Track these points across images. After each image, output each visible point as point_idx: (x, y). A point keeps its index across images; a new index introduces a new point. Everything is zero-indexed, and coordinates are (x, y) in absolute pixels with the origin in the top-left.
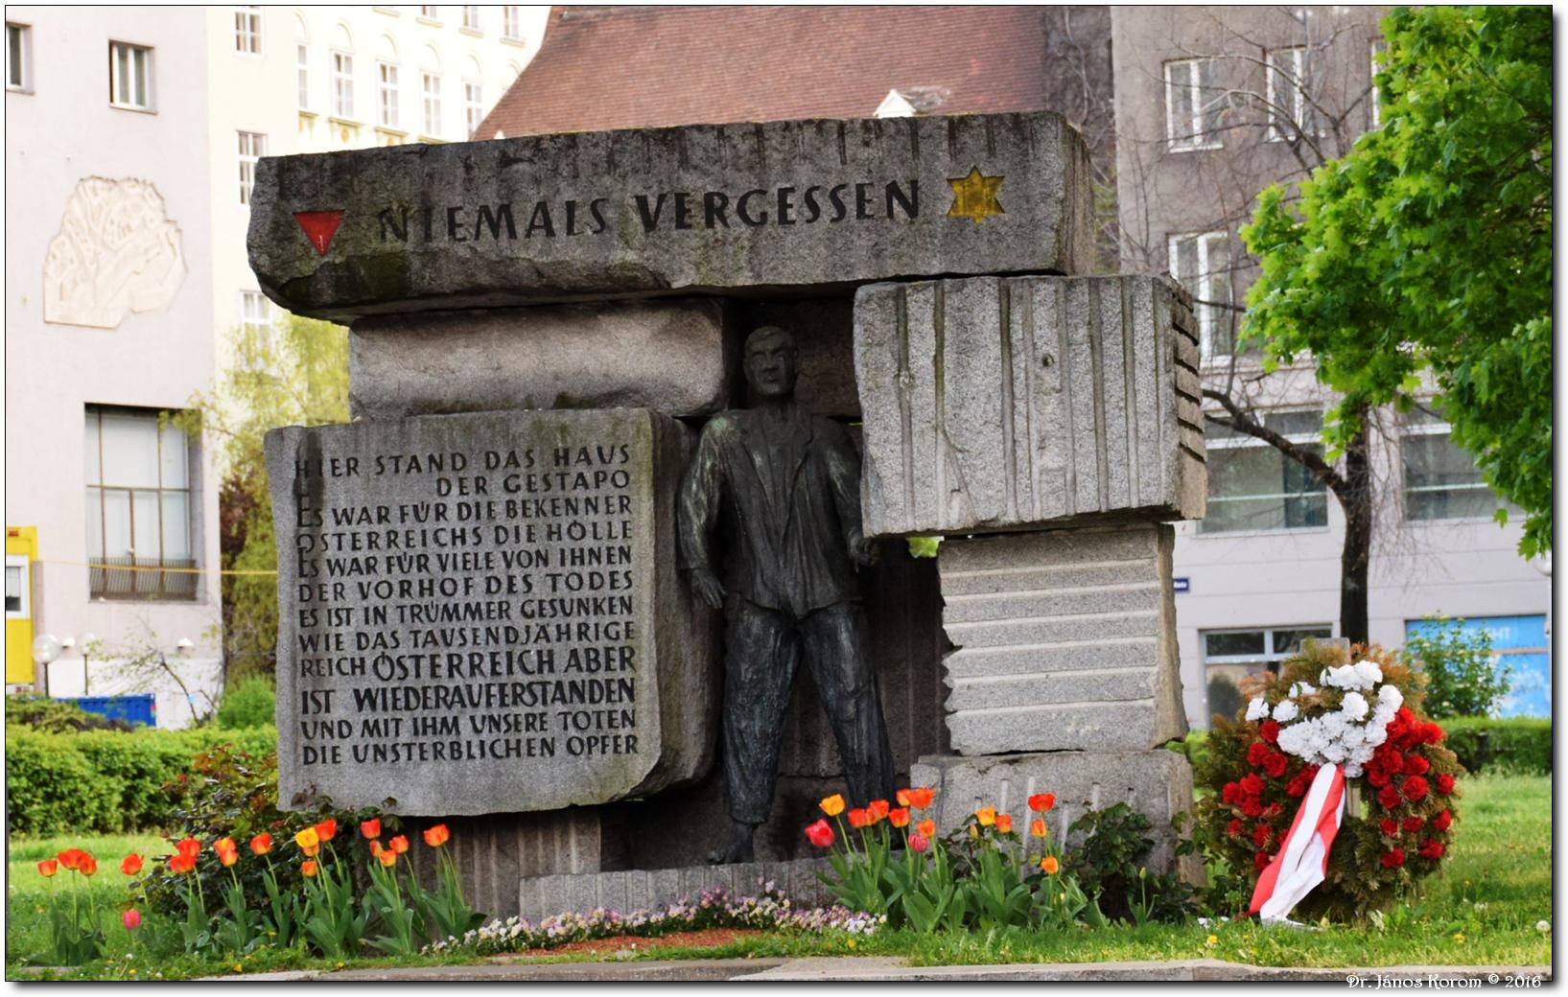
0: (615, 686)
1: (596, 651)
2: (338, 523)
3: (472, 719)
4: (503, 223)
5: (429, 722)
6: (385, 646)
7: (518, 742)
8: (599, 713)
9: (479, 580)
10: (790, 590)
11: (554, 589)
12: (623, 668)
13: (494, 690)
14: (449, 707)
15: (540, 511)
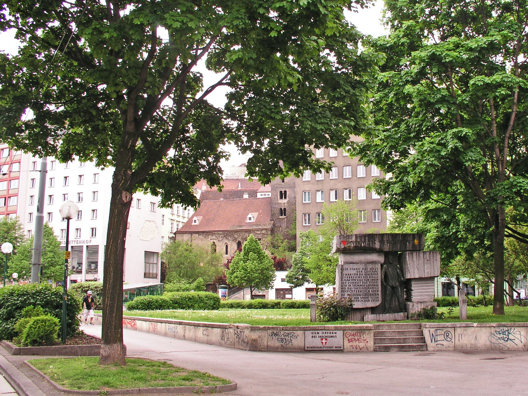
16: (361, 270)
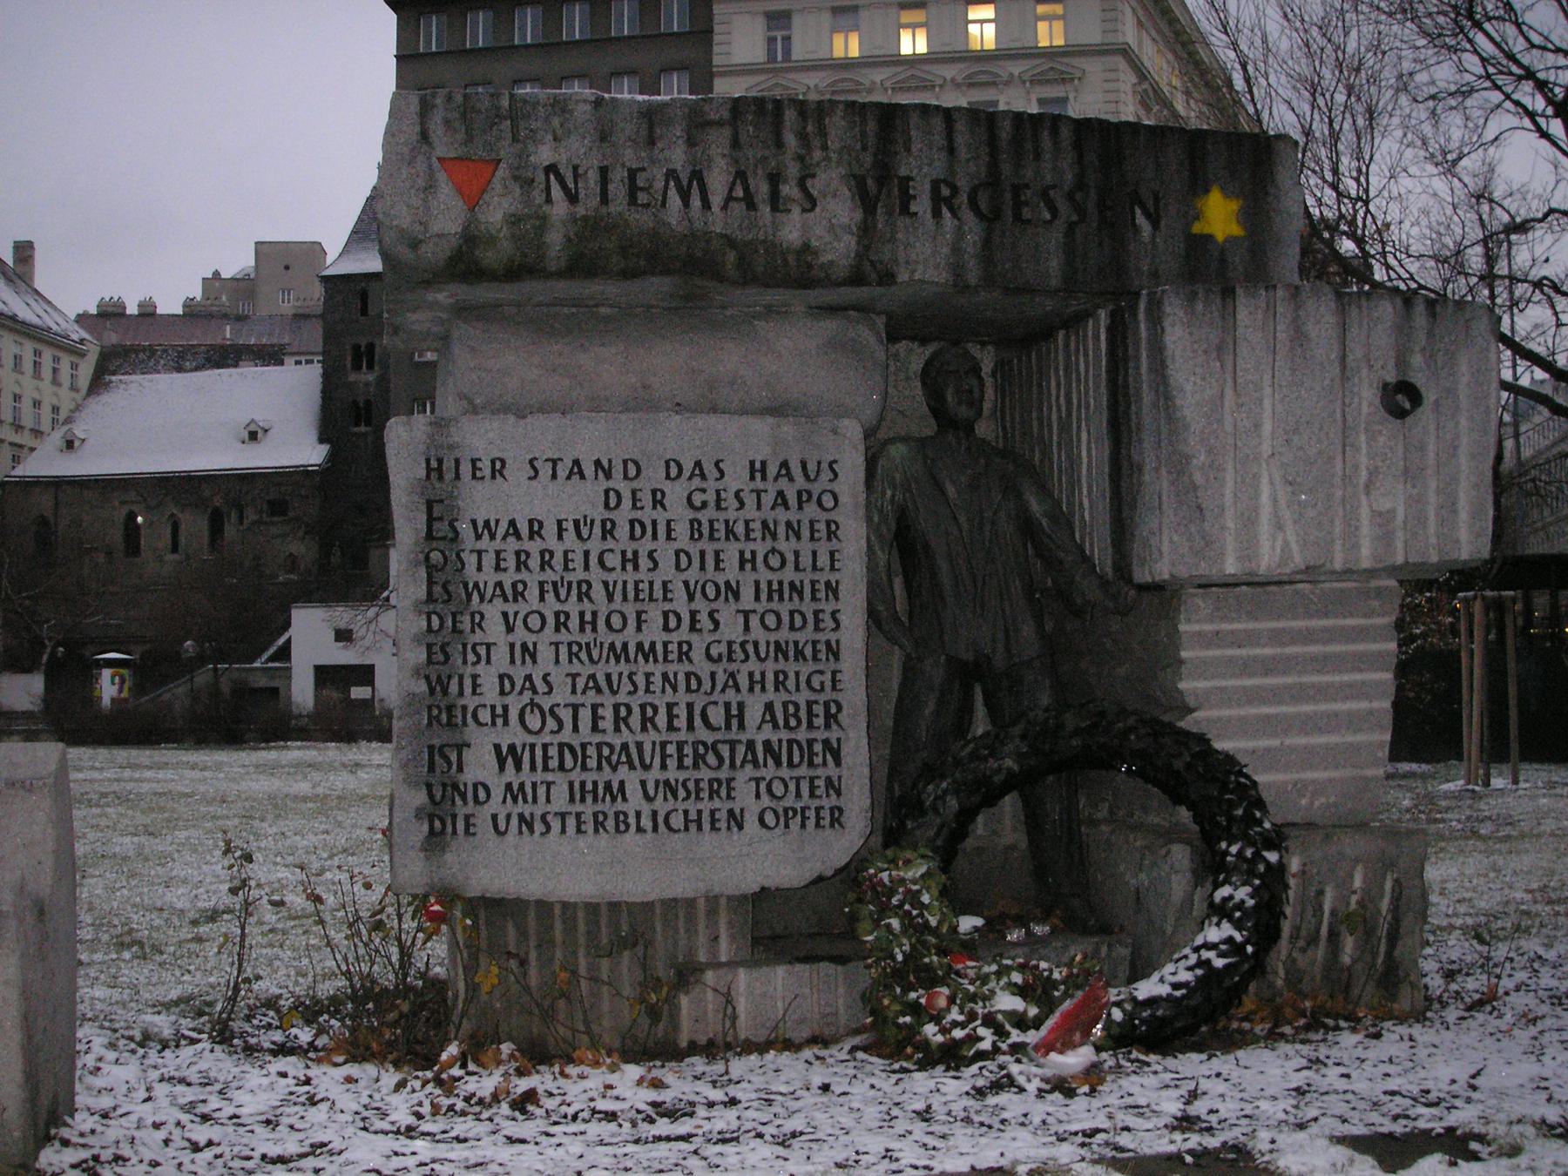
0: (818, 748)
1: (797, 706)
2: (478, 537)
3: (643, 783)
5: (589, 787)
6: (535, 692)
7: (700, 812)
8: (798, 780)
9: (654, 615)
11: (747, 628)
12: (827, 726)
14: (614, 769)
15: (730, 533)
16: (655, 475)
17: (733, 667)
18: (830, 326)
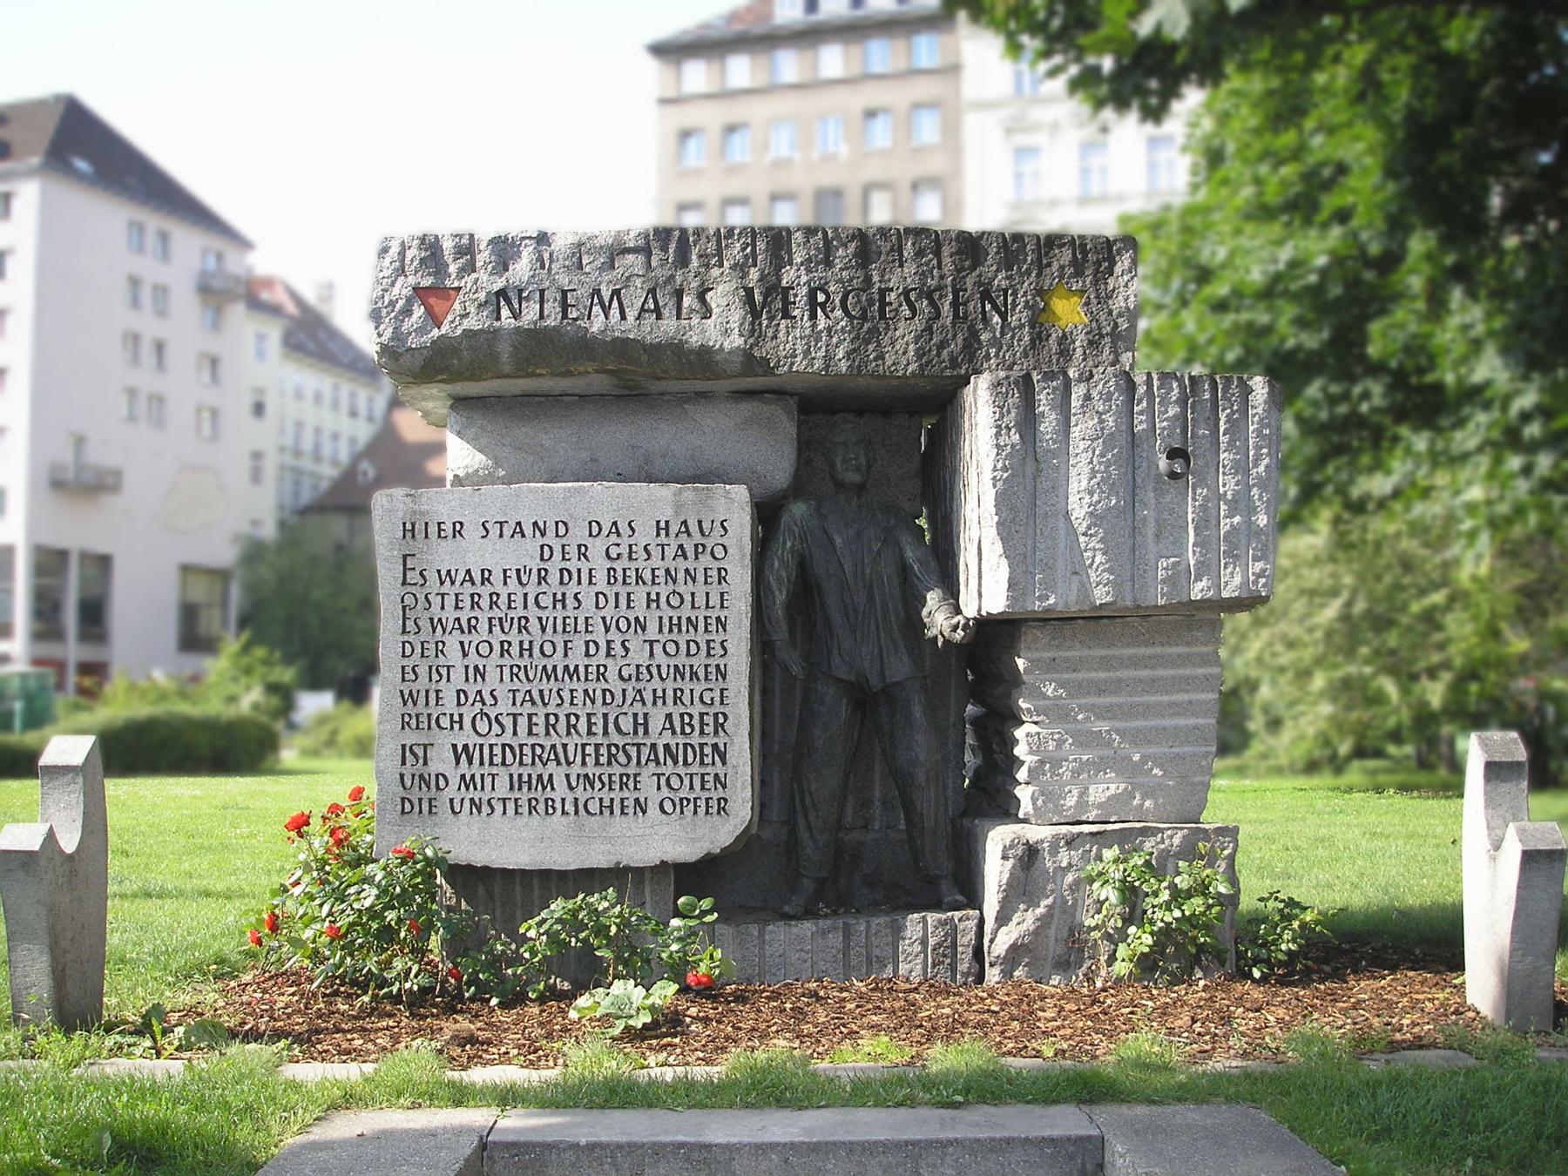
0: (708, 750)
1: (691, 716)
2: (442, 583)
3: (567, 776)
4: (615, 303)
5: (525, 778)
9: (578, 644)
10: (866, 664)
13: (590, 750)
14: (545, 765)
15: (639, 577)
16: (579, 534)
17: (640, 686)
18: (746, 408)
